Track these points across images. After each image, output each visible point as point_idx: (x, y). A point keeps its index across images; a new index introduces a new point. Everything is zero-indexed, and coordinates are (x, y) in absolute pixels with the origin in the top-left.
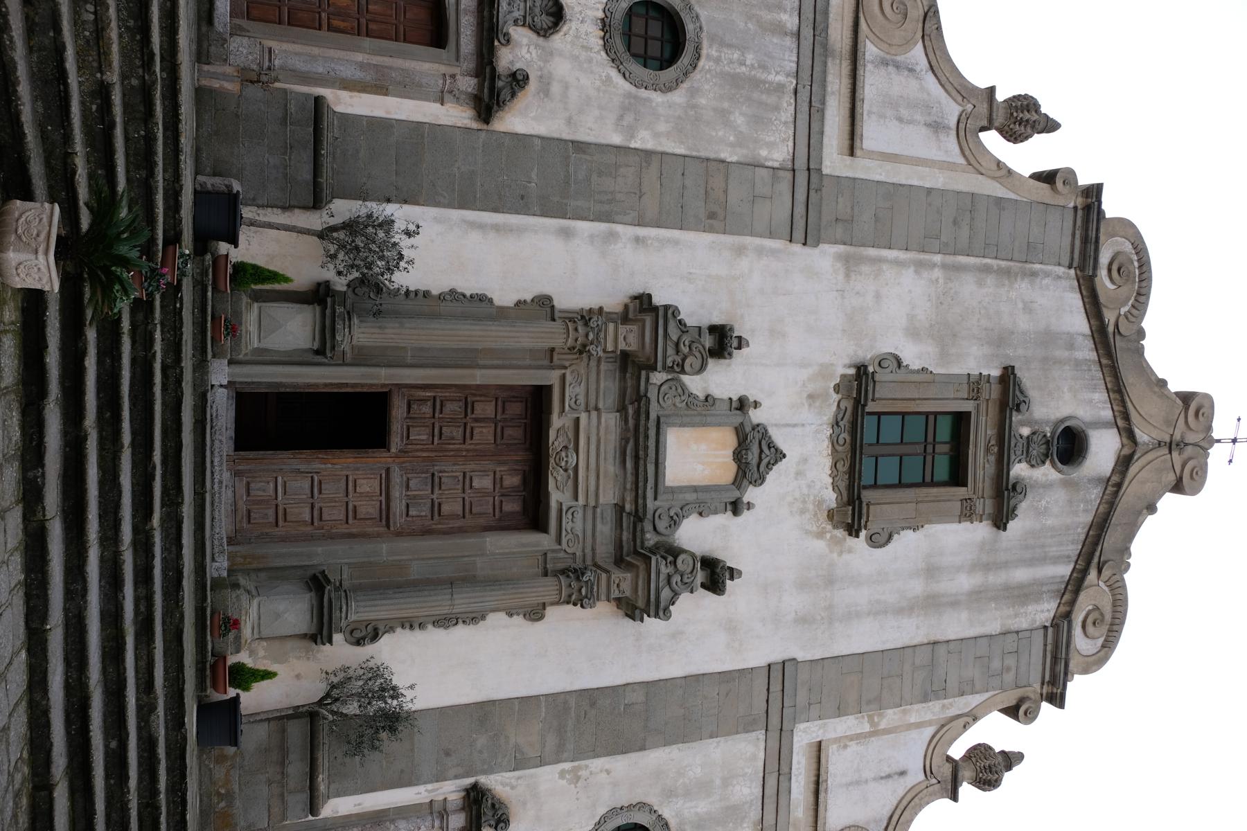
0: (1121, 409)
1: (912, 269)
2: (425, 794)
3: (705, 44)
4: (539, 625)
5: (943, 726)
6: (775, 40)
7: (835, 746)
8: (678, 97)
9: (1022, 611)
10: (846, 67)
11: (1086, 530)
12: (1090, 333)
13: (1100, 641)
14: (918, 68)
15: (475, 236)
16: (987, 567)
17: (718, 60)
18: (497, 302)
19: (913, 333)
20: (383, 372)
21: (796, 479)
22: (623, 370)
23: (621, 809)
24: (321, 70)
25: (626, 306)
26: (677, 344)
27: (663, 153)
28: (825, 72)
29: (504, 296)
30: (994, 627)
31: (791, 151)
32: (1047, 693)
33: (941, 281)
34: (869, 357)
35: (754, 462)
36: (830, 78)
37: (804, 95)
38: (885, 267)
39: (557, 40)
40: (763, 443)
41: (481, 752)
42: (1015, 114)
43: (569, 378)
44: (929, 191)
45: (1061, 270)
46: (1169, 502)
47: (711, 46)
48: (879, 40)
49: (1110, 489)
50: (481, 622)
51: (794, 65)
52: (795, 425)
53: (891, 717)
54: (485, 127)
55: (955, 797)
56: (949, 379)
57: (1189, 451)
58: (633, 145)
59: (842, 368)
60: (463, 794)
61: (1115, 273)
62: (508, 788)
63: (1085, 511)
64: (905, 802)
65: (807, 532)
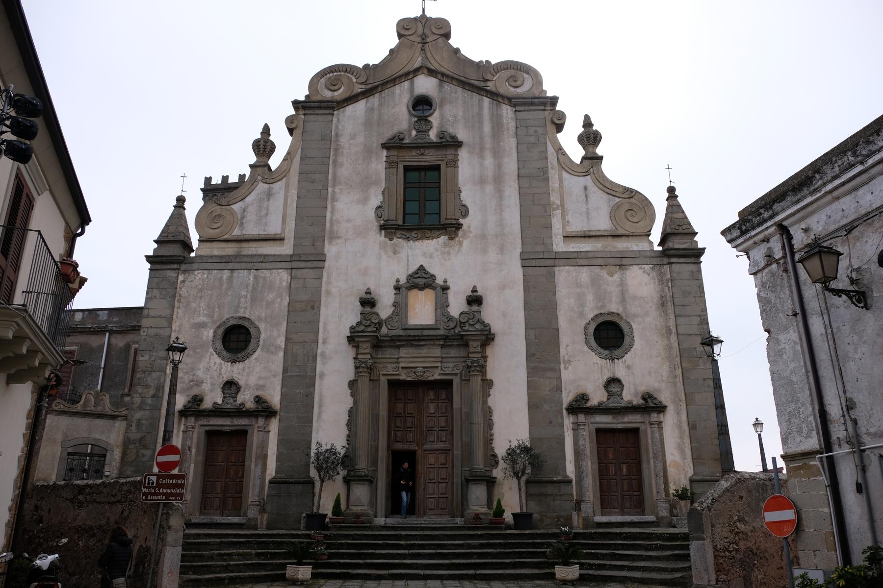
0: (403, 77)
1: (335, 203)
2: (569, 433)
3: (239, 315)
4: (495, 382)
5: (562, 167)
6: (235, 281)
7: (567, 228)
8: (262, 326)
9: (506, 126)
10: (245, 245)
11: (466, 91)
12: (365, 99)
13: (526, 76)
14: (243, 207)
15: (324, 416)
16: (482, 149)
17: (245, 308)
18: (351, 405)
19: (365, 201)
20: (380, 454)
21: (433, 258)
22: (381, 347)
23: (586, 339)
24: (259, 482)
25: (353, 346)
26: (366, 326)
27: (287, 332)
28: (248, 256)
29: (349, 402)
30: (513, 142)
31: (283, 270)
32: (551, 106)
33: (341, 187)
34: (376, 224)
35: (424, 280)
36: (250, 253)
37: (259, 265)
38: (334, 218)
39: (241, 383)
40: (415, 276)
41: (551, 407)
42: (261, 152)
43: (384, 372)
44: (299, 197)
45: (335, 119)
46: (454, 42)
47: (239, 312)
48: (232, 228)
49: (445, 79)
50: (492, 408)
51: (246, 271)
52: (408, 260)
53: (555, 199)
54: (278, 413)
55: (601, 158)
56: (388, 179)
57: (427, 31)
58: (284, 347)
59: (382, 238)
60: (571, 415)
61: (336, 88)
62: (570, 394)
63: (456, 93)
64: (601, 186)
65: (459, 251)
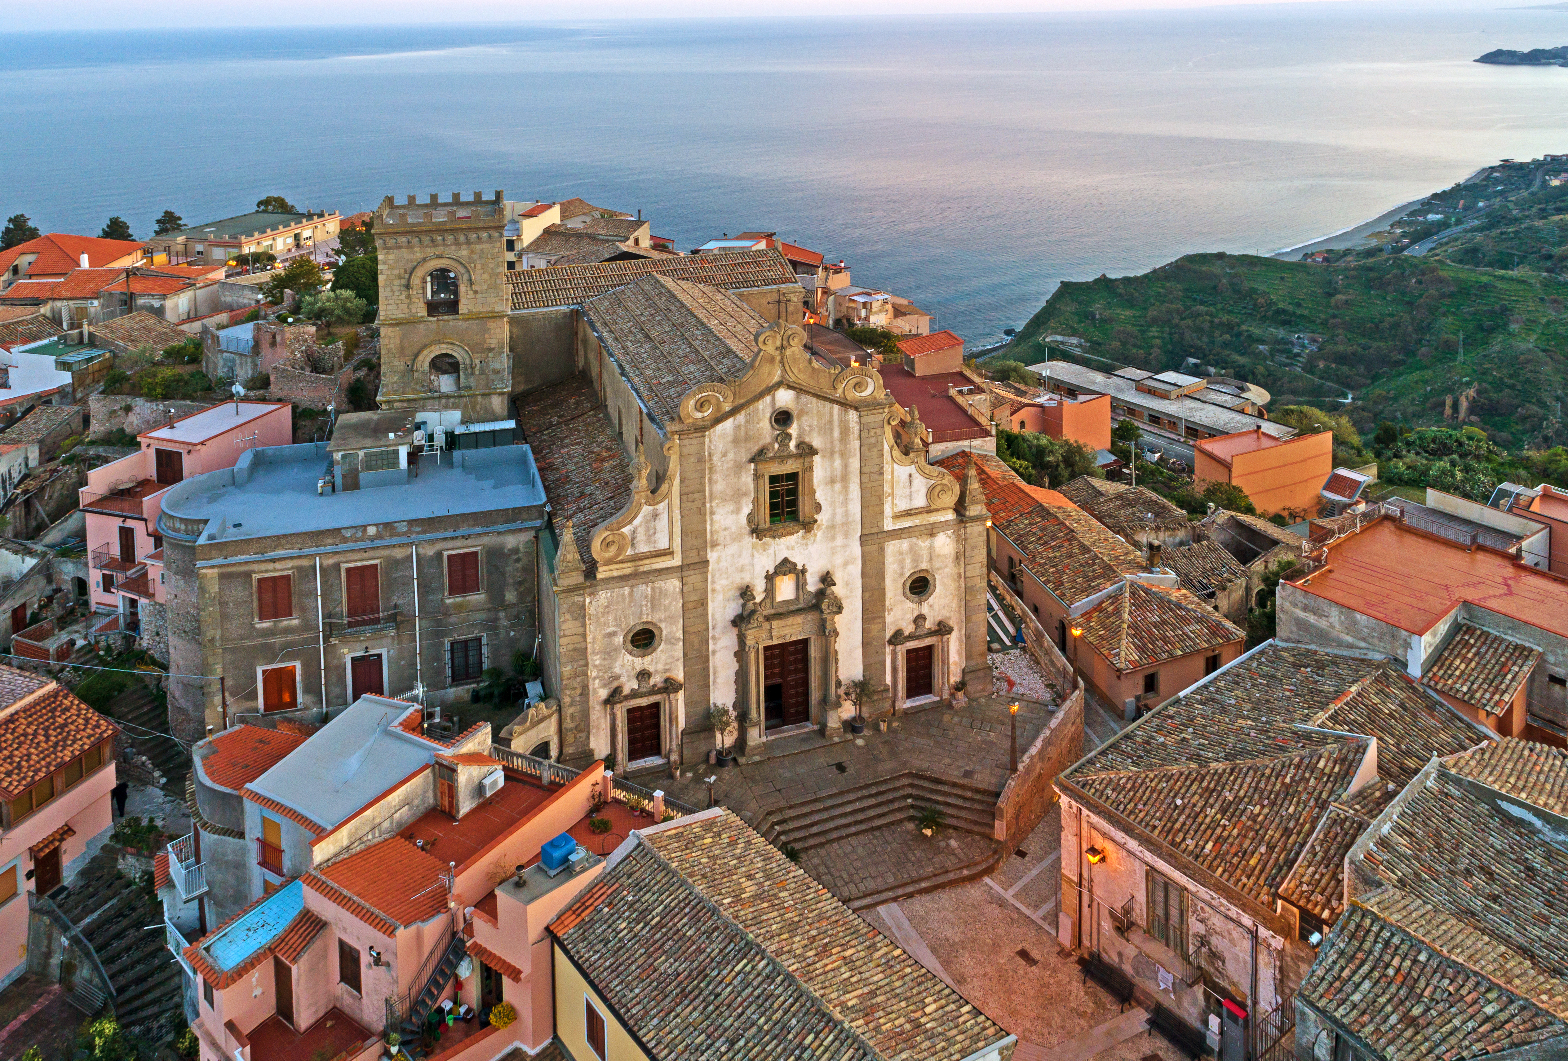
19: (738, 511)
